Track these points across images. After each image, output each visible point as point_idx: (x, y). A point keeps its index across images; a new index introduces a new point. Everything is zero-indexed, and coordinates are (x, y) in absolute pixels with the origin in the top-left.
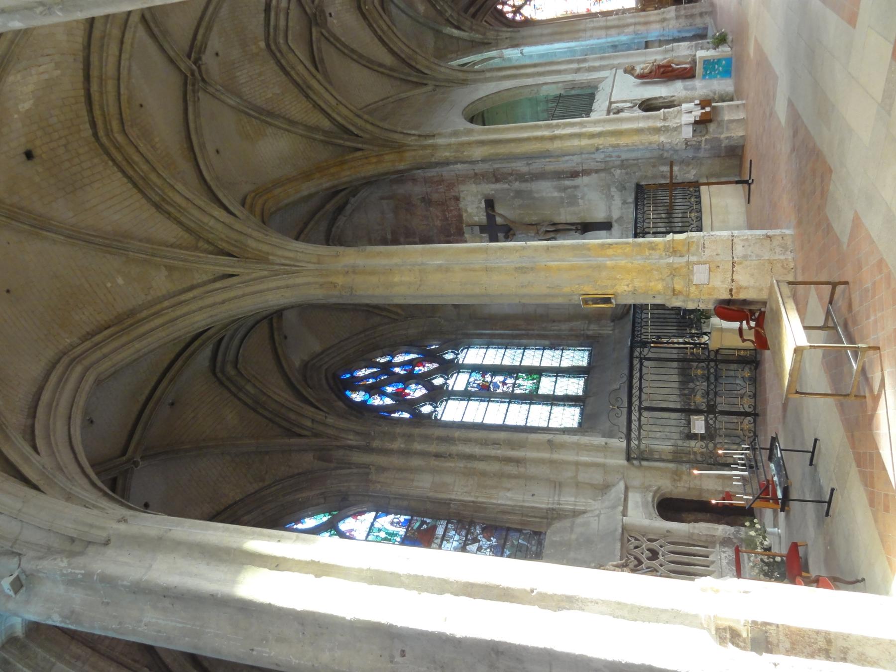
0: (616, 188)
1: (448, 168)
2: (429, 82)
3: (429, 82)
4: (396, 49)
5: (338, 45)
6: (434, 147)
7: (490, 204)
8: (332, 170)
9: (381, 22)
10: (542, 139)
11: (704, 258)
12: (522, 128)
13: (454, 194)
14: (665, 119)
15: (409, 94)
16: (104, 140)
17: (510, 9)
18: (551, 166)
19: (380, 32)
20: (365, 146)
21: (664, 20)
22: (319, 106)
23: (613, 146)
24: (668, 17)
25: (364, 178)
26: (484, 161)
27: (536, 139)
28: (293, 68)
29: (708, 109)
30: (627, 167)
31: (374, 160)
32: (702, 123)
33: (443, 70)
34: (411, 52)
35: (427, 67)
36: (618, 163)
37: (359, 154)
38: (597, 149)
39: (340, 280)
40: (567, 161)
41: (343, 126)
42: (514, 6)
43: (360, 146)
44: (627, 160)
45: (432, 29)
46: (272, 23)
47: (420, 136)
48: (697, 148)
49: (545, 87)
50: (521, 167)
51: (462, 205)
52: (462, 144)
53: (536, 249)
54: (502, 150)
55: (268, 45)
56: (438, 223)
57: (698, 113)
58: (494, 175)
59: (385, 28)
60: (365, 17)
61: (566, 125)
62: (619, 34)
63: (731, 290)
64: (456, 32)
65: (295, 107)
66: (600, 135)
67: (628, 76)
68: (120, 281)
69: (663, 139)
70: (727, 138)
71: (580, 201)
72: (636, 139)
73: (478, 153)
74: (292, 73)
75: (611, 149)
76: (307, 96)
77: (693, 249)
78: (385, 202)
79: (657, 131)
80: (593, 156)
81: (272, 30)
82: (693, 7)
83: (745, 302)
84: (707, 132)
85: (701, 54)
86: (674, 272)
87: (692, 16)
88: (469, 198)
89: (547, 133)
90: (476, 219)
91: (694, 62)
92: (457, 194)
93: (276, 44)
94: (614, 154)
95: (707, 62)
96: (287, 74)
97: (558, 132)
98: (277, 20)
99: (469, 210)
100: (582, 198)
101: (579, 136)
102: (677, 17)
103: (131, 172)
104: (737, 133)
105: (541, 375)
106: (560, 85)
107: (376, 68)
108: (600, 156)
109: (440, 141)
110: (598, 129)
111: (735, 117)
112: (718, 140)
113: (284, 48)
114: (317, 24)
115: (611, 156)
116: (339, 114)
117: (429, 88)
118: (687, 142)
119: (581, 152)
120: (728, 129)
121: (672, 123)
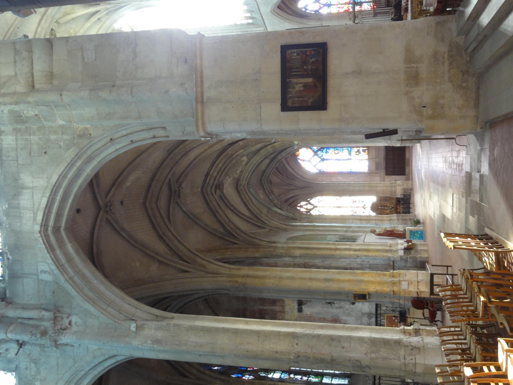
1: (281, 259)
2: (266, 227)
3: (266, 227)
4: (252, 210)
5: (226, 201)
6: (276, 248)
8: (222, 251)
9: (246, 196)
10: (330, 249)
11: (406, 279)
12: (321, 244)
14: (390, 247)
15: (256, 231)
16: (148, 205)
17: (305, 210)
18: (334, 264)
19: (245, 200)
20: (239, 243)
21: (391, 220)
22: (220, 221)
23: (366, 256)
24: (393, 218)
25: (237, 258)
26: (300, 257)
27: (328, 249)
28: (211, 202)
29: (410, 244)
31: (243, 250)
32: (408, 250)
33: (274, 222)
34: (259, 212)
35: (267, 220)
36: (368, 266)
37: (236, 246)
38: (358, 256)
39: (240, 280)
41: (230, 232)
42: (307, 209)
43: (237, 242)
44: (372, 264)
45: (266, 206)
46: (207, 181)
47: (268, 242)
48: (406, 261)
49: (329, 236)
50: (318, 262)
52: (290, 248)
53: (333, 273)
54: (310, 252)
55: (202, 191)
57: (406, 245)
59: (248, 199)
60: (239, 192)
61: (343, 245)
62: (367, 223)
63: (417, 293)
64: (279, 211)
65: (208, 219)
66: (359, 250)
67: (373, 234)
68: (138, 264)
69: (389, 255)
70: (420, 257)
72: (377, 254)
73: (298, 252)
74: (211, 204)
75: (364, 257)
76: (215, 215)
77: (401, 276)
79: (387, 251)
80: (355, 260)
81: (206, 185)
82: (406, 216)
83: (424, 298)
84: (410, 254)
85: (409, 228)
86: (394, 283)
87: (405, 220)
89: (333, 247)
91: (405, 230)
93: (206, 190)
94: (366, 260)
95: (411, 232)
96: (208, 204)
97: (339, 247)
98: (210, 180)
101: (349, 250)
102: (398, 219)
103: (153, 220)
104: (424, 255)
105: (323, 377)
106: (337, 236)
107: (241, 215)
108: (359, 261)
109: (279, 245)
110: (358, 247)
111: (423, 248)
112: (416, 258)
113: (209, 192)
114: (220, 189)
115: (364, 261)
116: (228, 226)
117: (267, 230)
118: (401, 257)
119: (350, 257)
120: (420, 253)
121: (394, 248)
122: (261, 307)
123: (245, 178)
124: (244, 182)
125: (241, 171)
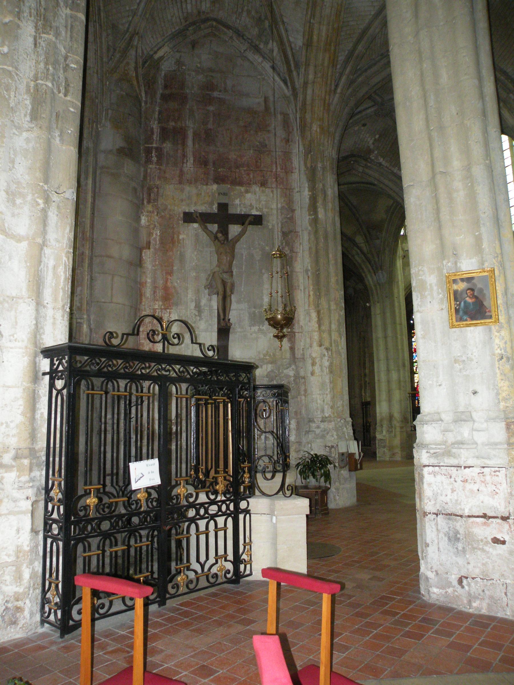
0: (272, 371)
7: (258, 220)
13: (269, 181)
30: (296, 383)
40: (308, 314)
51: (256, 188)
56: (233, 156)
58: (291, 232)
71: (256, 328)
78: (262, 100)
88: (263, 198)
90: (237, 202)
92: (269, 185)
99: (248, 196)
100: (259, 330)
115: (313, 364)
122: (190, 134)
123: (367, 171)
124: (361, 169)
125: (380, 164)
